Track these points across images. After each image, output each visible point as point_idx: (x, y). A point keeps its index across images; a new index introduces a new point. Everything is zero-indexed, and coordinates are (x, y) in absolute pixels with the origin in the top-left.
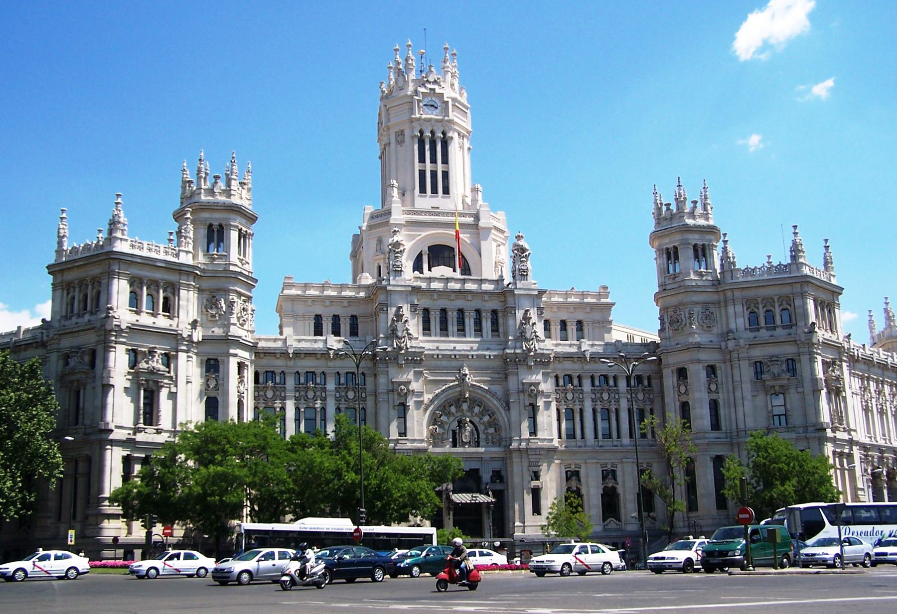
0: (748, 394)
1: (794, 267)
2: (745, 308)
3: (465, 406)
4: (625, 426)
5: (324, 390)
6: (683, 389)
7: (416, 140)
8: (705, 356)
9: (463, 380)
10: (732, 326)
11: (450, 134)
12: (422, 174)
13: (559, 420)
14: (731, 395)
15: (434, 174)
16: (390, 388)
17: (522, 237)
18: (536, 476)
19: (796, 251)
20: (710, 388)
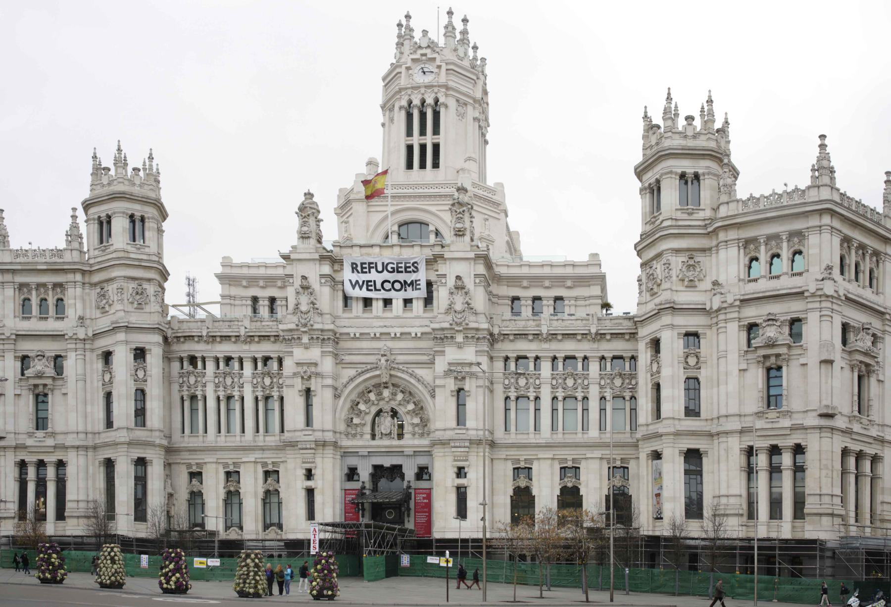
0: (734, 369)
3: (386, 393)
9: (380, 360)
14: (715, 370)
20: (687, 362)
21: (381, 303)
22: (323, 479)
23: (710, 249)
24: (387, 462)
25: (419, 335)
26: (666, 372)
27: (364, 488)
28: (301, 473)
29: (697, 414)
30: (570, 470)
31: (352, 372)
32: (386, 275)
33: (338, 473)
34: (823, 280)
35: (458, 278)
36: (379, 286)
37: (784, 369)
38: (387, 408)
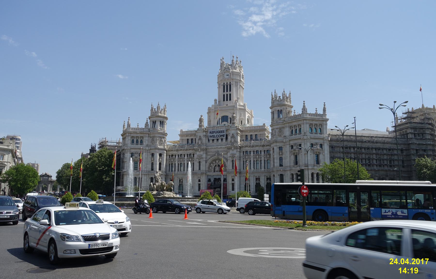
1: (302, 115)
2: (290, 128)
3: (217, 161)
4: (263, 164)
5: (184, 159)
6: (274, 154)
7: (222, 87)
8: (278, 144)
10: (286, 135)
11: (232, 83)
12: (224, 95)
13: (244, 164)
15: (227, 95)
16: (197, 157)
17: (235, 113)
18: (233, 180)
19: (304, 109)
21: (216, 140)
22: (203, 182)
23: (284, 127)
24: (217, 177)
25: (224, 148)
26: (275, 156)
27: (212, 183)
28: (197, 180)
29: (282, 166)
30: (258, 179)
31: (209, 157)
32: (217, 134)
33: (206, 180)
34: (304, 135)
35: (232, 134)
36: (215, 136)
37: (298, 156)
38: (217, 165)
